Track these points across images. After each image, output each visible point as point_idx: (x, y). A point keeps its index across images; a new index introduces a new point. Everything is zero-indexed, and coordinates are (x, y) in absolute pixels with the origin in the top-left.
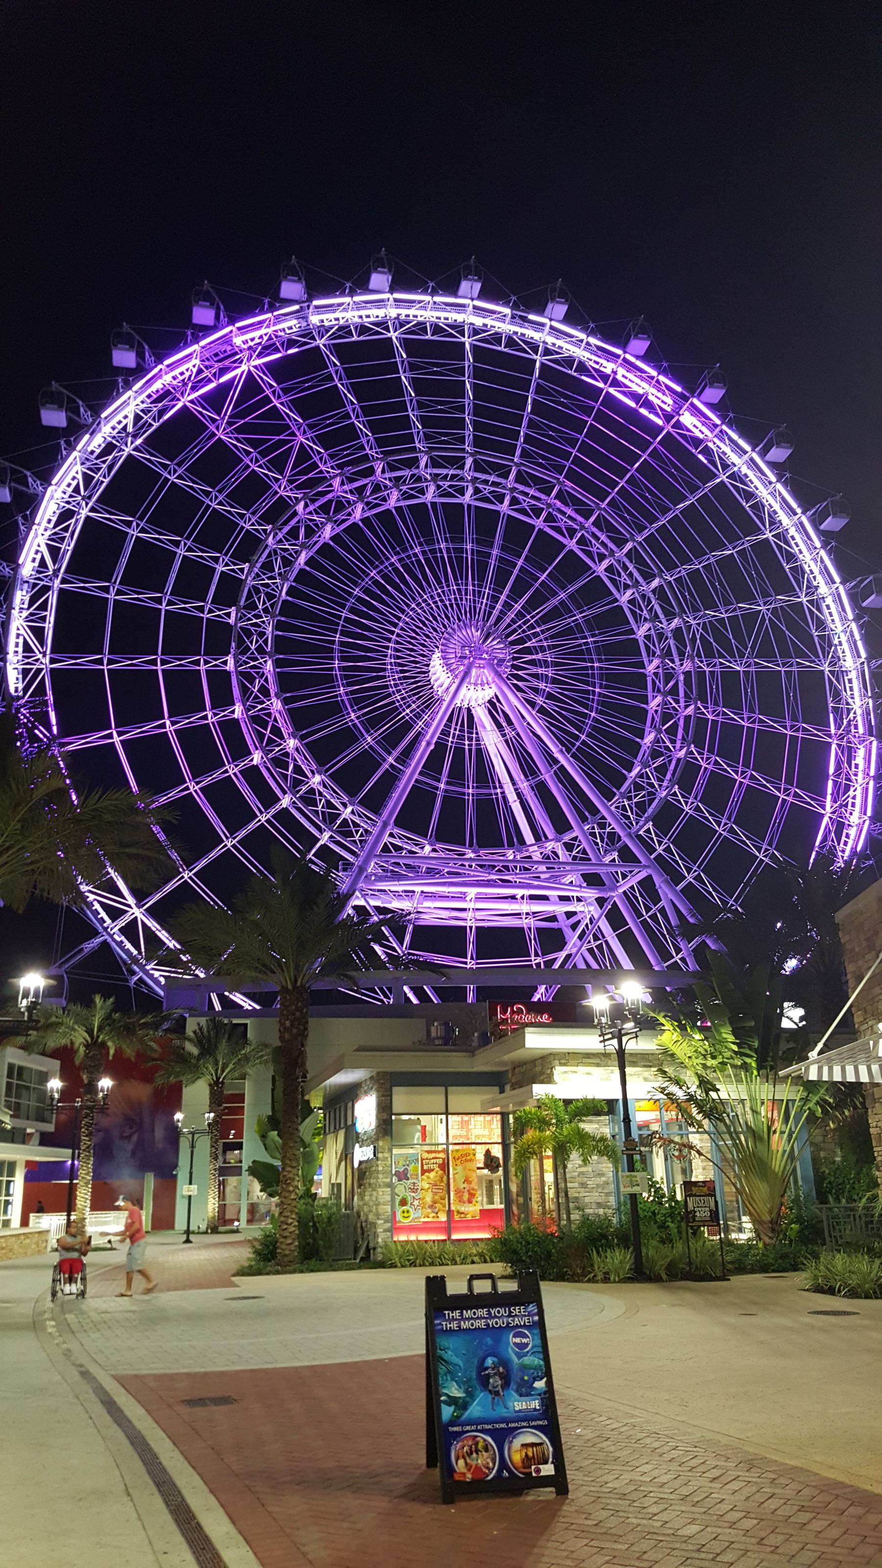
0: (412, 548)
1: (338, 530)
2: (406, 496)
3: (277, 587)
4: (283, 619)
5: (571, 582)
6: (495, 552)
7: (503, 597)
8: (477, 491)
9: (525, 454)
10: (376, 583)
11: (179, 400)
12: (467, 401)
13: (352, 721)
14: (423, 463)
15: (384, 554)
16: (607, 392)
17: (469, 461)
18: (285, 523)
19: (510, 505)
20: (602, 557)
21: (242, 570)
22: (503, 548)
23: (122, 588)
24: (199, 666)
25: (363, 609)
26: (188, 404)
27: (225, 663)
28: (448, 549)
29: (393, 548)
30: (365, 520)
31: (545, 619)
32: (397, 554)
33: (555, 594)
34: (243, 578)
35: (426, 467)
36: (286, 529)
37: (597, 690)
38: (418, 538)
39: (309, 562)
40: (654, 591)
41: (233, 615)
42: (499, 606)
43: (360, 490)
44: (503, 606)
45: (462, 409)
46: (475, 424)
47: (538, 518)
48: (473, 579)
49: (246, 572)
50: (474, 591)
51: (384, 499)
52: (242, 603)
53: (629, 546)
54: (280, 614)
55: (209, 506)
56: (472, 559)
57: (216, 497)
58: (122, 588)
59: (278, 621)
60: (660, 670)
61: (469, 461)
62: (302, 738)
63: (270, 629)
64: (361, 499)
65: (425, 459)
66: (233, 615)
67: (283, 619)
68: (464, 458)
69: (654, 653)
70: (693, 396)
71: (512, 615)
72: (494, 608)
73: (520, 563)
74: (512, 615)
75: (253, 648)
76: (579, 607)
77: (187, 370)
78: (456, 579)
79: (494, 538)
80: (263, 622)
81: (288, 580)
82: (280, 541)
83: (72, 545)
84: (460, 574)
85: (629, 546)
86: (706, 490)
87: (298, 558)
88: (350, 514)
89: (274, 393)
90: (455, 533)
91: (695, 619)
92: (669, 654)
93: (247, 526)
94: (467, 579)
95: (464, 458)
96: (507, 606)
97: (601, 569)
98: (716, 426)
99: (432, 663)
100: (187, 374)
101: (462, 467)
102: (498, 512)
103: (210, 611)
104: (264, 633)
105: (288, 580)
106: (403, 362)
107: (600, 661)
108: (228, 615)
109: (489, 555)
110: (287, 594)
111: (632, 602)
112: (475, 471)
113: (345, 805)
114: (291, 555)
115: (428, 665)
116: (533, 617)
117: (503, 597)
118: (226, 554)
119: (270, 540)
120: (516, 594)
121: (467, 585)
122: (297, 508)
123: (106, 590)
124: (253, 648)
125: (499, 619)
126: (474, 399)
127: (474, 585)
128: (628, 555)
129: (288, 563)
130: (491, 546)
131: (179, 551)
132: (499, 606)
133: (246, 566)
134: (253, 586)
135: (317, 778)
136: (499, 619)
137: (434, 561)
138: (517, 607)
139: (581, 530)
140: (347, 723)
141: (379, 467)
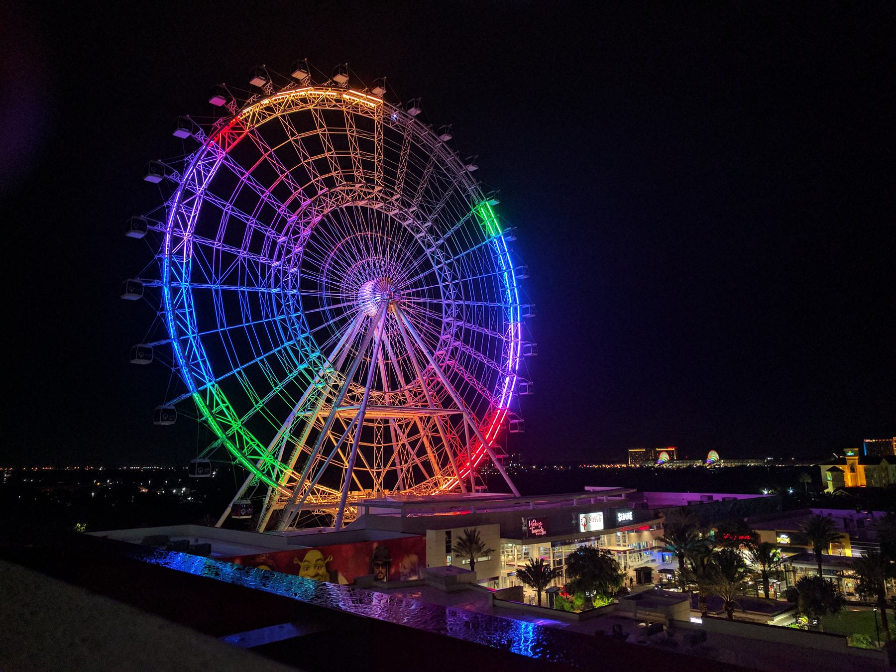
3: (345, 199)
4: (339, 211)
13: (324, 268)
24: (295, 191)
27: (305, 200)
31: (419, 304)
41: (323, 191)
52: (332, 191)
59: (337, 209)
62: (306, 253)
63: (329, 210)
66: (323, 191)
67: (339, 211)
83: (296, 110)
96: (407, 288)
108: (322, 189)
110: (346, 207)
113: (294, 288)
116: (414, 299)
133: (344, 183)
135: (294, 270)
138: (411, 291)
140: (320, 266)
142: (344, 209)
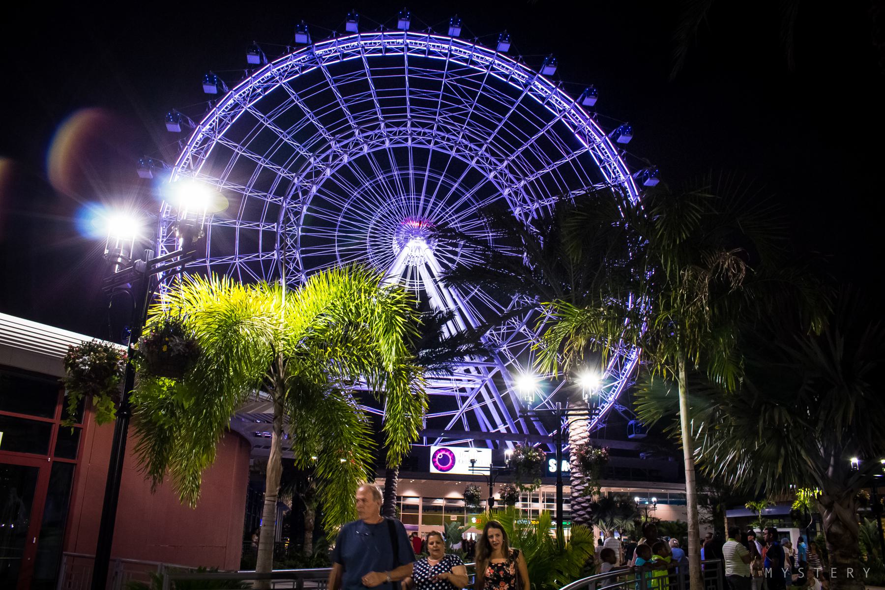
0: (364, 184)
1: (318, 187)
2: (351, 155)
5: (458, 178)
6: (411, 172)
7: (422, 197)
8: (391, 140)
9: (412, 111)
10: (348, 209)
11: (214, 140)
12: (372, 91)
14: (357, 133)
15: (350, 193)
16: (449, 61)
17: (382, 125)
18: (303, 171)
19: (412, 141)
20: (472, 158)
21: (274, 227)
22: (415, 169)
23: (212, 259)
25: (355, 204)
26: (219, 141)
28: (384, 178)
29: (354, 189)
30: (333, 175)
32: (356, 190)
33: (452, 186)
34: (275, 230)
35: (359, 134)
36: (304, 174)
37: (490, 234)
38: (366, 178)
39: (319, 191)
40: (506, 167)
42: (422, 202)
43: (326, 159)
44: (424, 202)
45: (370, 96)
46: (380, 101)
47: (430, 144)
48: (403, 193)
49: (276, 227)
50: (405, 198)
51: (341, 160)
53: (485, 146)
54: (301, 246)
55: (246, 195)
56: (399, 179)
57: (248, 190)
58: (212, 259)
60: (521, 212)
61: (382, 125)
64: (328, 166)
65: (358, 131)
68: (379, 124)
69: (516, 204)
70: (538, 73)
71: (430, 205)
72: (419, 203)
73: (427, 173)
74: (430, 205)
75: (292, 268)
76: (469, 199)
77: (214, 122)
78: (393, 196)
79: (409, 165)
80: (294, 253)
81: (300, 225)
82: (289, 203)
84: (396, 193)
85: (485, 146)
86: (575, 156)
87: (302, 210)
88: (324, 175)
89: (264, 120)
90: (385, 167)
91: (548, 202)
92: (525, 201)
93: (269, 200)
94: (400, 194)
95: (379, 124)
97: (473, 163)
98: (514, 64)
99: (393, 246)
100: (214, 124)
101: (380, 128)
102: (407, 147)
103: (262, 256)
104: (295, 258)
105: (300, 225)
106: (330, 80)
107: (492, 232)
109: (408, 174)
111: (495, 177)
112: (387, 128)
114: (308, 188)
115: (392, 244)
117: (422, 197)
118: (262, 222)
119: (284, 205)
120: (429, 193)
121: (401, 196)
122: (310, 160)
123: (205, 262)
124: (292, 268)
125: (424, 209)
126: (375, 89)
127: (404, 196)
128: (486, 151)
129: (297, 214)
130: (408, 169)
131: (236, 226)
132: (422, 202)
134: (282, 233)
136: (424, 209)
137: (378, 186)
139: (456, 145)
141: (332, 143)
142: (318, 194)
